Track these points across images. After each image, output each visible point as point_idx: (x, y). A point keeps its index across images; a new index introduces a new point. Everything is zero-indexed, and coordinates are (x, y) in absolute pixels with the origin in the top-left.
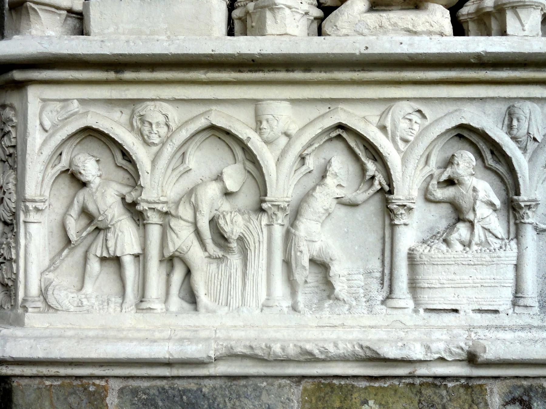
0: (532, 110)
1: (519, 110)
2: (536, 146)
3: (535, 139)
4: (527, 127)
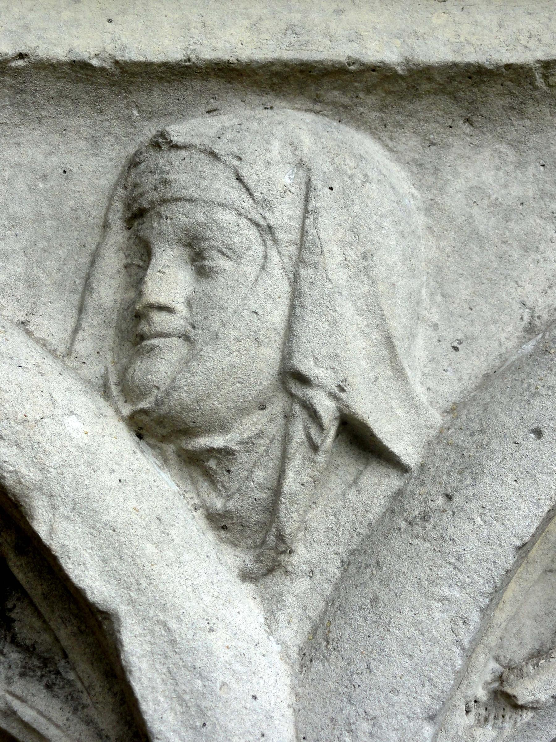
0: (322, 166)
1: (206, 167)
2: (378, 507)
3: (358, 439)
4: (277, 315)
